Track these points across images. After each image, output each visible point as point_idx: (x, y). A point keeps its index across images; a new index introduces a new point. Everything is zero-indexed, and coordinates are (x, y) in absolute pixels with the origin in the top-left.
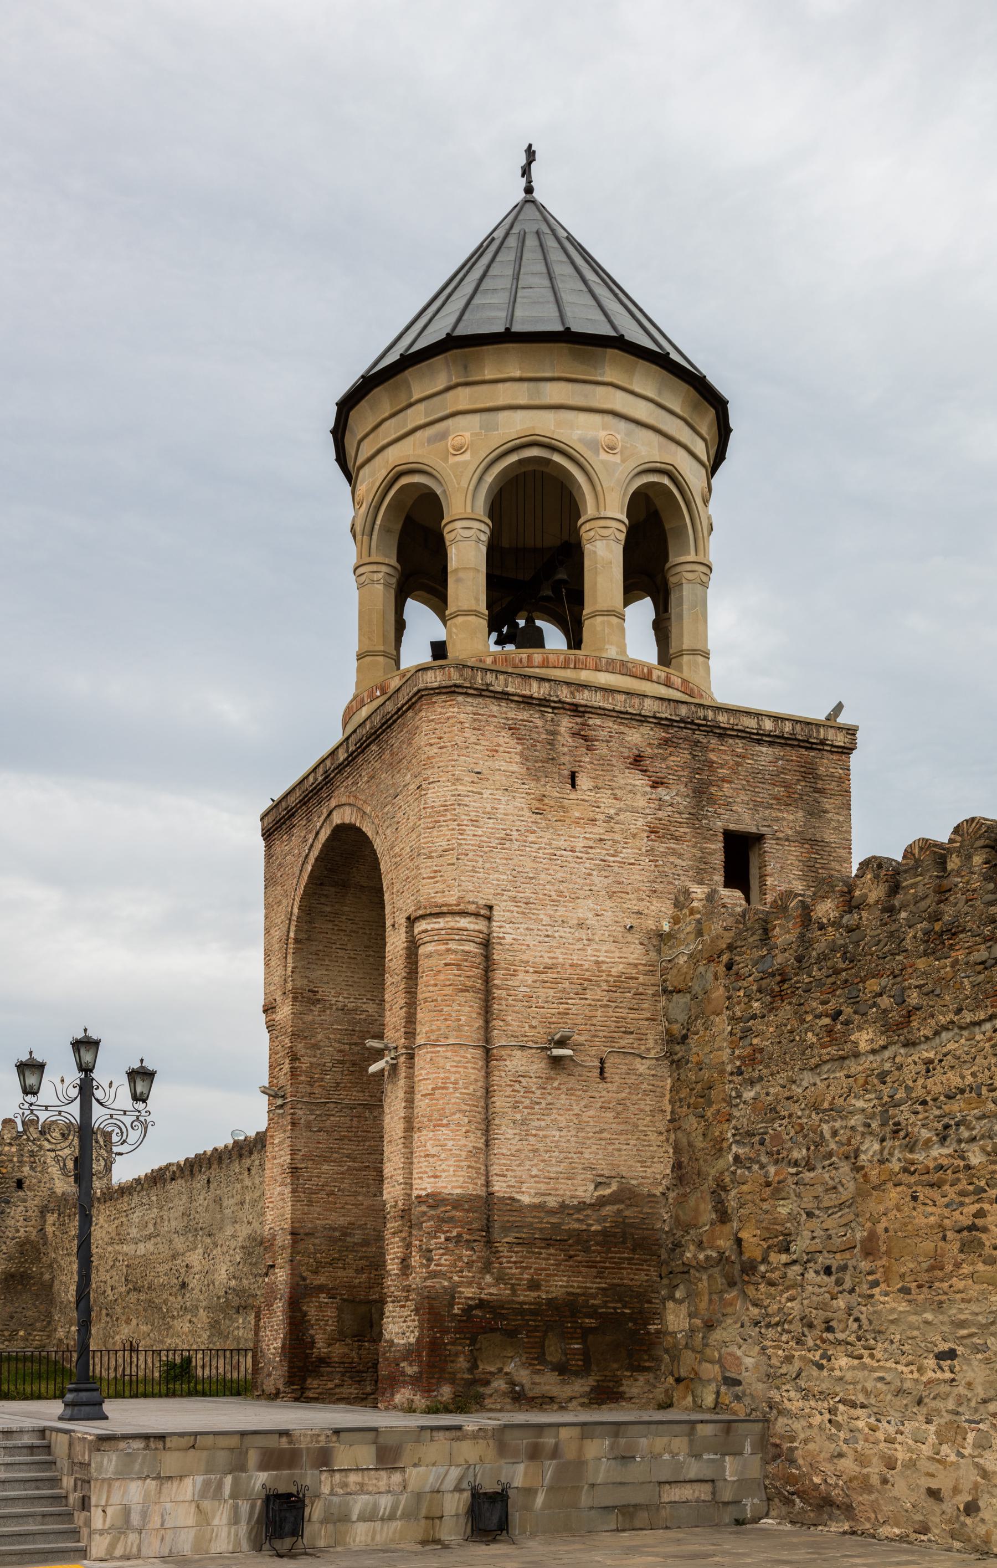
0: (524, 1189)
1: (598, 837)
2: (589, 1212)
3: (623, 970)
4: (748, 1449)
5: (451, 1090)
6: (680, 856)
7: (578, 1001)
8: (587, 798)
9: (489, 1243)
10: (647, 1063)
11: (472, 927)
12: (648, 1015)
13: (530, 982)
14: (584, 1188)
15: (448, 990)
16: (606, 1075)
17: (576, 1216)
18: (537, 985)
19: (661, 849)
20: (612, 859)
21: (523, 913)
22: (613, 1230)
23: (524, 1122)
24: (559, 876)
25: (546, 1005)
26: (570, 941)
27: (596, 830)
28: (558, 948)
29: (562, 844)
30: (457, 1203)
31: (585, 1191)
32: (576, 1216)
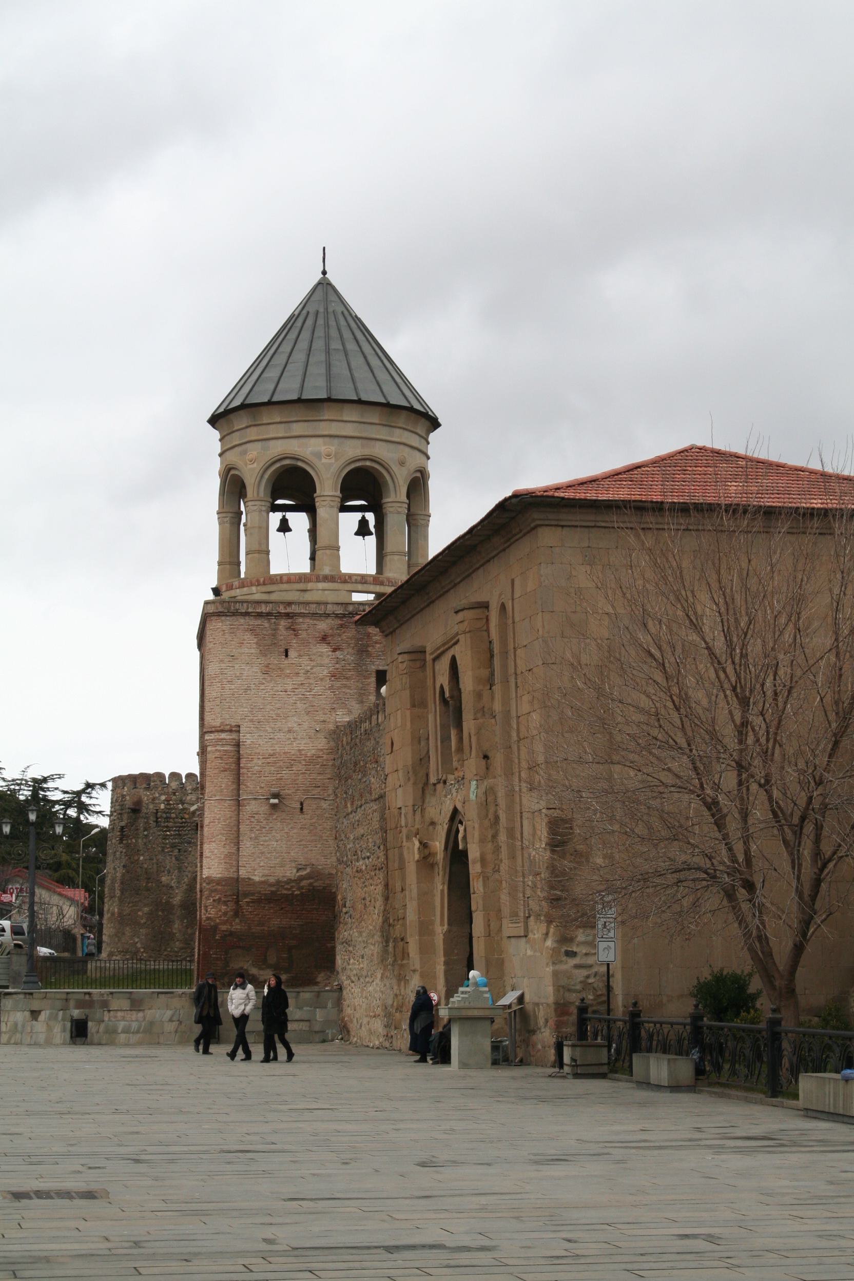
2: (293, 884)
4: (330, 1005)
6: (349, 688)
9: (237, 902)
10: (328, 802)
11: (228, 737)
12: (329, 777)
23: (256, 838)
24: (277, 706)
27: (300, 679)
29: (280, 688)
30: (219, 882)
31: (290, 872)
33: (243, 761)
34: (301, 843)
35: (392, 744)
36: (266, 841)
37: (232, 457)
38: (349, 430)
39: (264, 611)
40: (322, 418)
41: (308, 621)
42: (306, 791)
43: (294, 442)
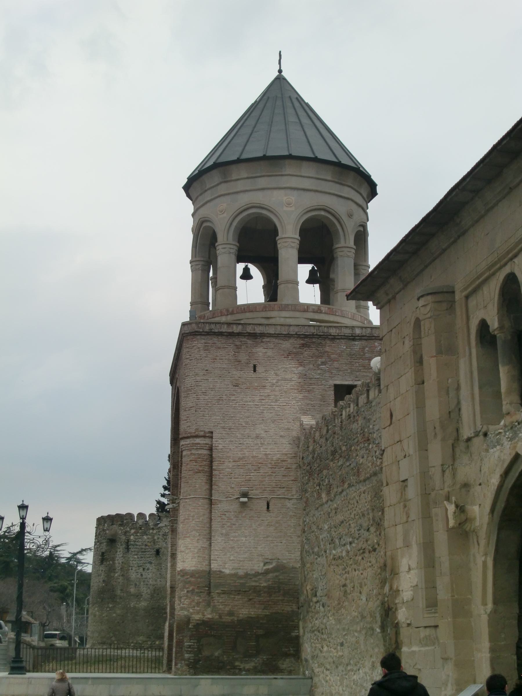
0: (226, 567)
1: (266, 394)
2: (261, 577)
3: (280, 457)
5: (191, 520)
7: (256, 474)
8: (261, 376)
9: (209, 593)
10: (292, 502)
11: (202, 442)
12: (293, 478)
13: (231, 466)
14: (258, 565)
15: (191, 473)
16: (270, 509)
17: (253, 579)
18: (235, 467)
19: (300, 397)
20: (274, 404)
21: (228, 434)
22: (273, 585)
23: (227, 535)
25: (239, 477)
26: (252, 445)
27: (267, 391)
28: (246, 449)
30: (193, 574)
31: (259, 567)
32: (253, 579)
33: (215, 464)
34: (268, 539)
35: (391, 415)
36: (235, 537)
37: (204, 212)
38: (306, 184)
39: (235, 332)
40: (283, 173)
41: (274, 340)
42: (273, 491)
43: (260, 194)
